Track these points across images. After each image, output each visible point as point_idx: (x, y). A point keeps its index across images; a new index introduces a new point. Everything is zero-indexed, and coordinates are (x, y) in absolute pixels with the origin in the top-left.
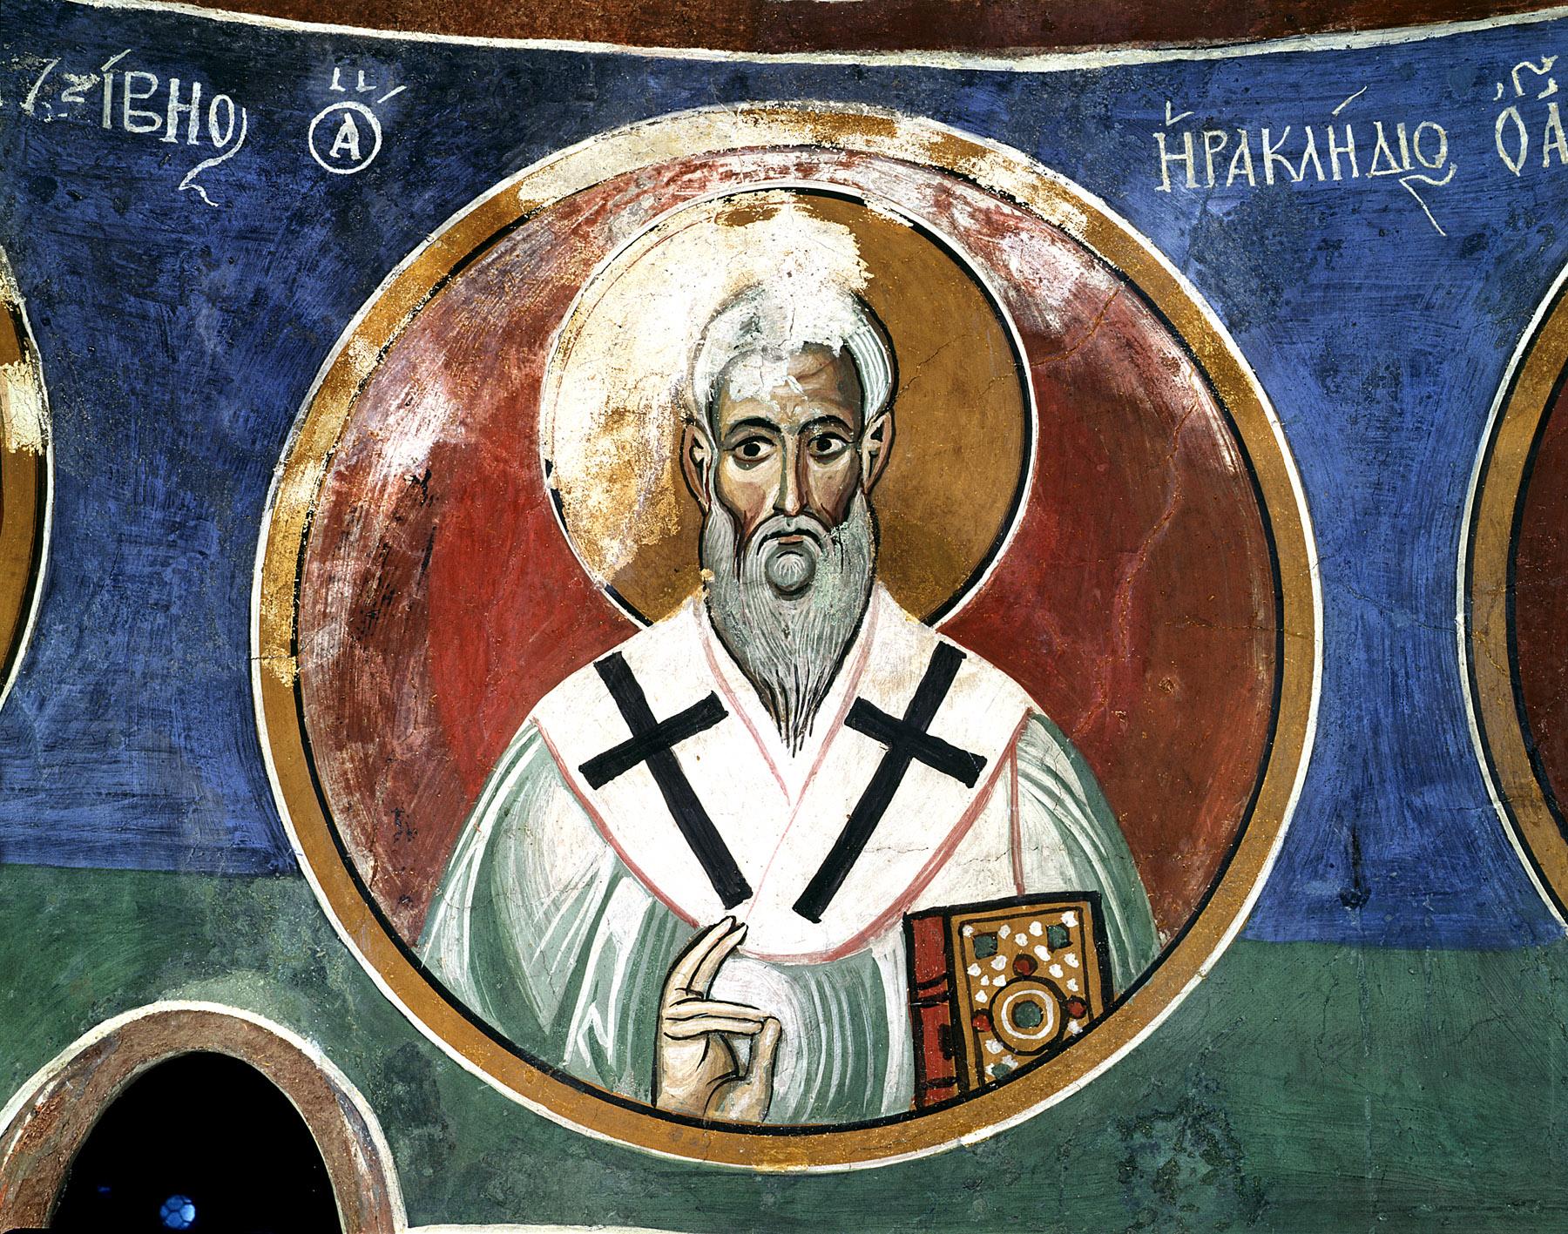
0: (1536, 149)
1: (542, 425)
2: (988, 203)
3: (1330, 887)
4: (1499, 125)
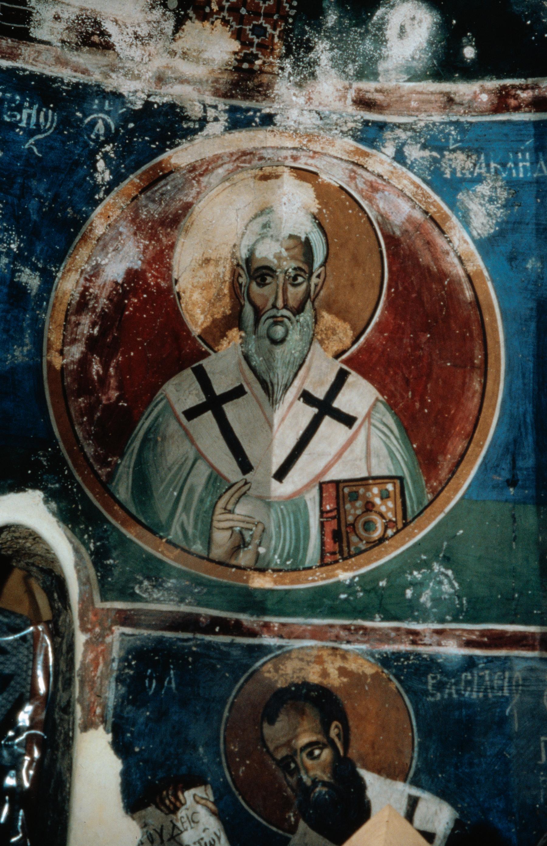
1: (174, 263)
2: (372, 178)
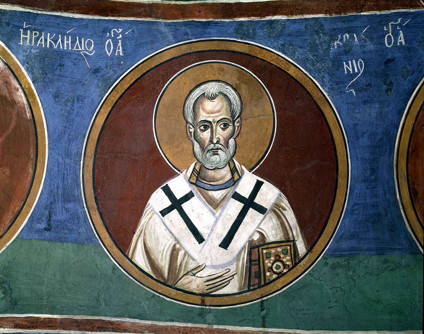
0: (114, 50)
3: (43, 226)
4: (107, 43)
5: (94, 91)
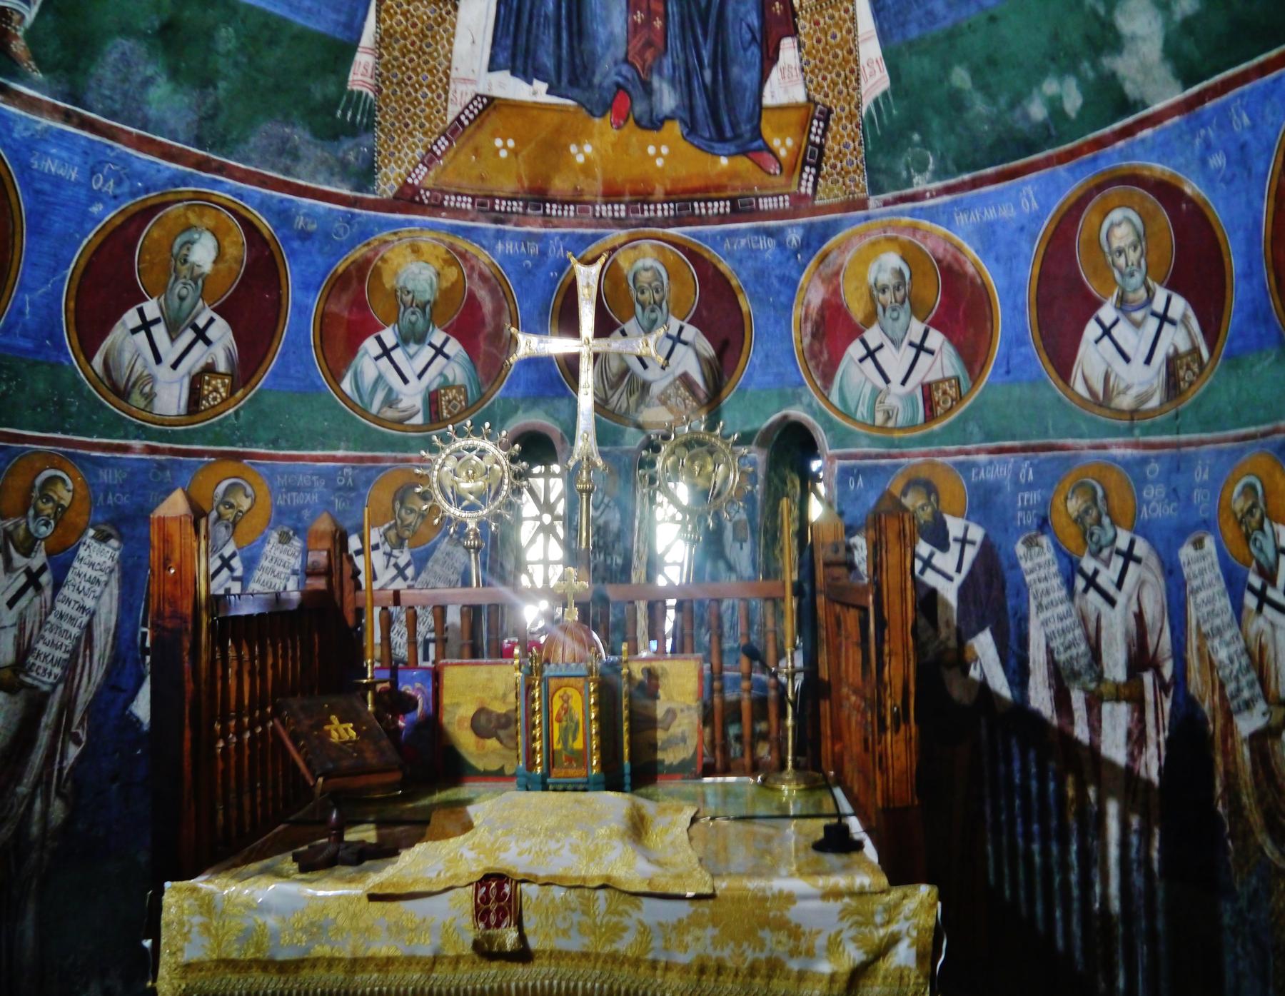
5: (1025, 245)
